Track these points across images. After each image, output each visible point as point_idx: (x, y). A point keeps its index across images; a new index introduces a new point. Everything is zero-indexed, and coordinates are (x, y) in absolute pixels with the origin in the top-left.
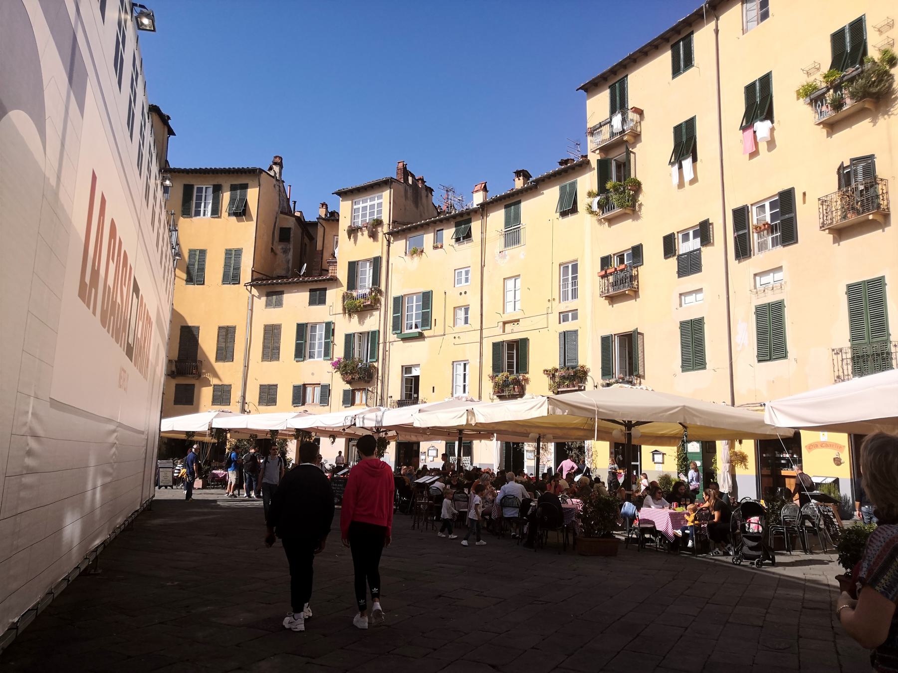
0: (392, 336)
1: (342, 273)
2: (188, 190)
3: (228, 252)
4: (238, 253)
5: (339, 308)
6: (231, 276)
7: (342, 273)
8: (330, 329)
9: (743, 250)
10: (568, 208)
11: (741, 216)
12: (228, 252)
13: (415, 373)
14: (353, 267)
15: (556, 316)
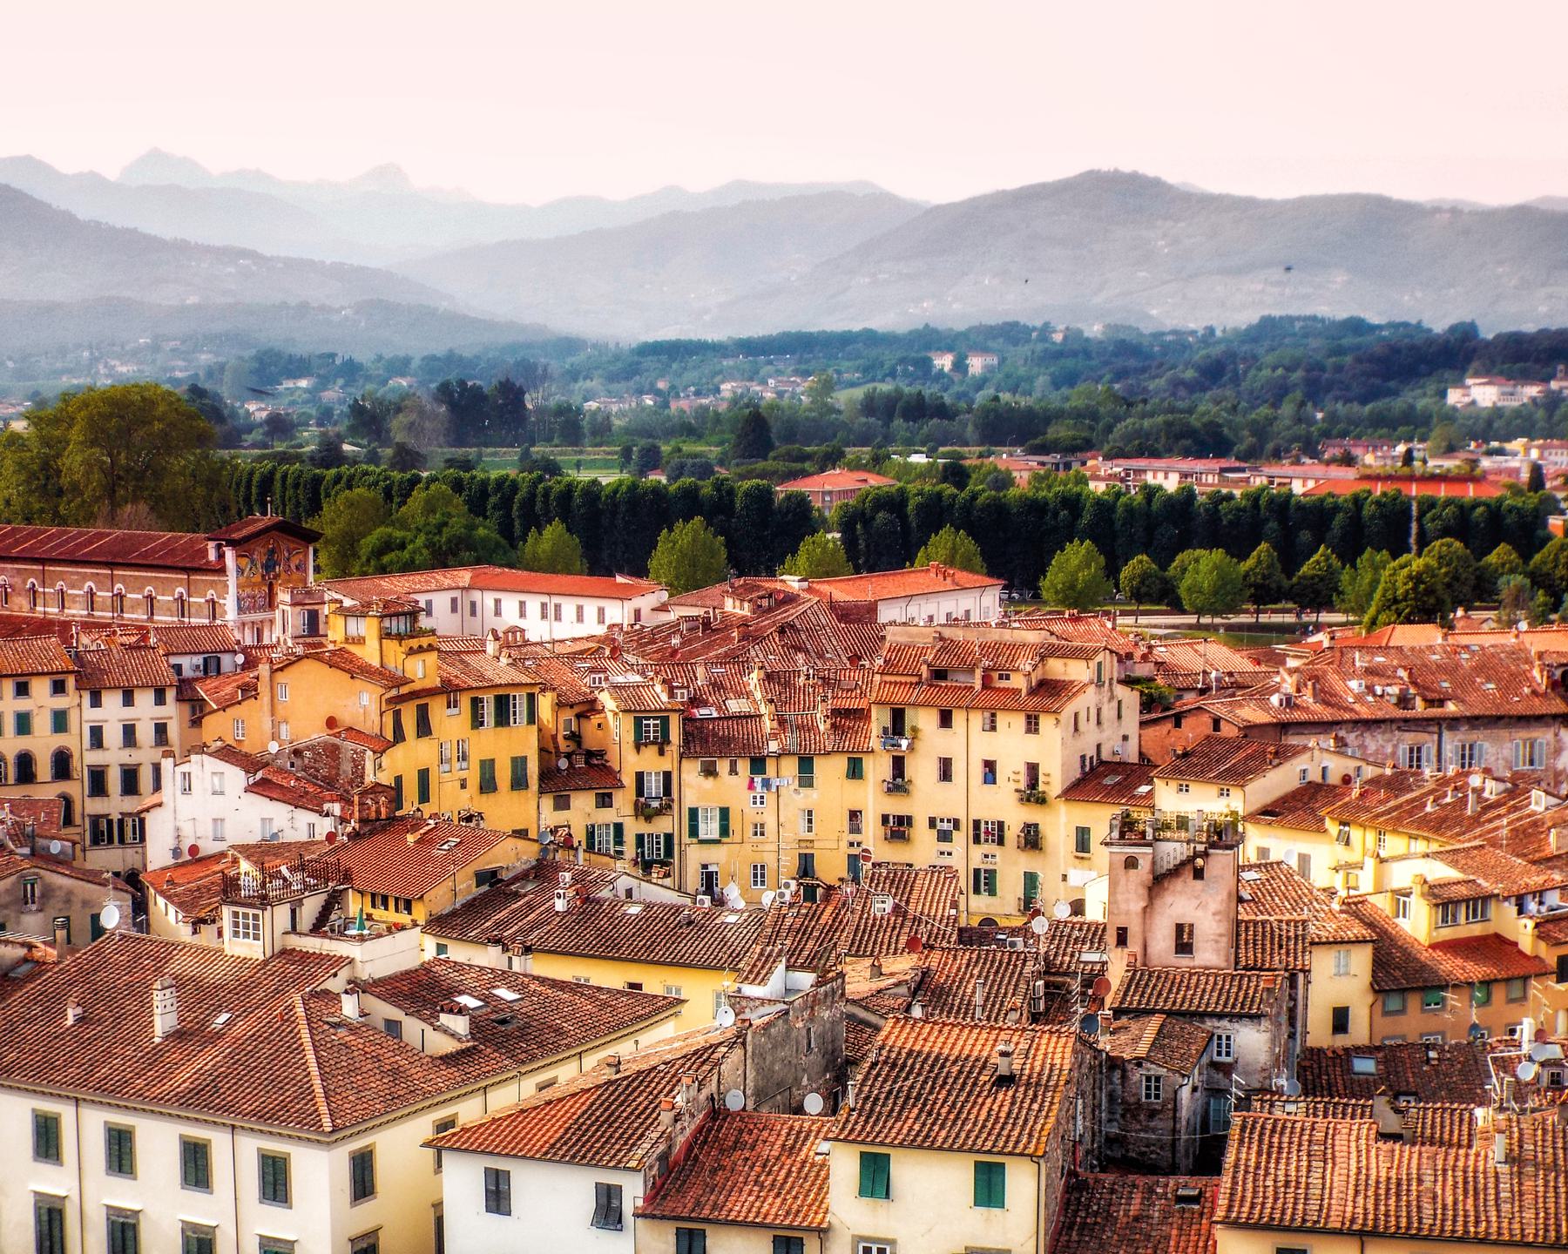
0: (686, 839)
1: (628, 780)
2: (476, 703)
3: (514, 760)
4: (524, 759)
5: (629, 810)
6: (519, 782)
7: (628, 780)
8: (619, 828)
9: (977, 840)
10: (855, 771)
11: (977, 824)
12: (514, 760)
13: (711, 869)
14: (640, 777)
15: (844, 844)
